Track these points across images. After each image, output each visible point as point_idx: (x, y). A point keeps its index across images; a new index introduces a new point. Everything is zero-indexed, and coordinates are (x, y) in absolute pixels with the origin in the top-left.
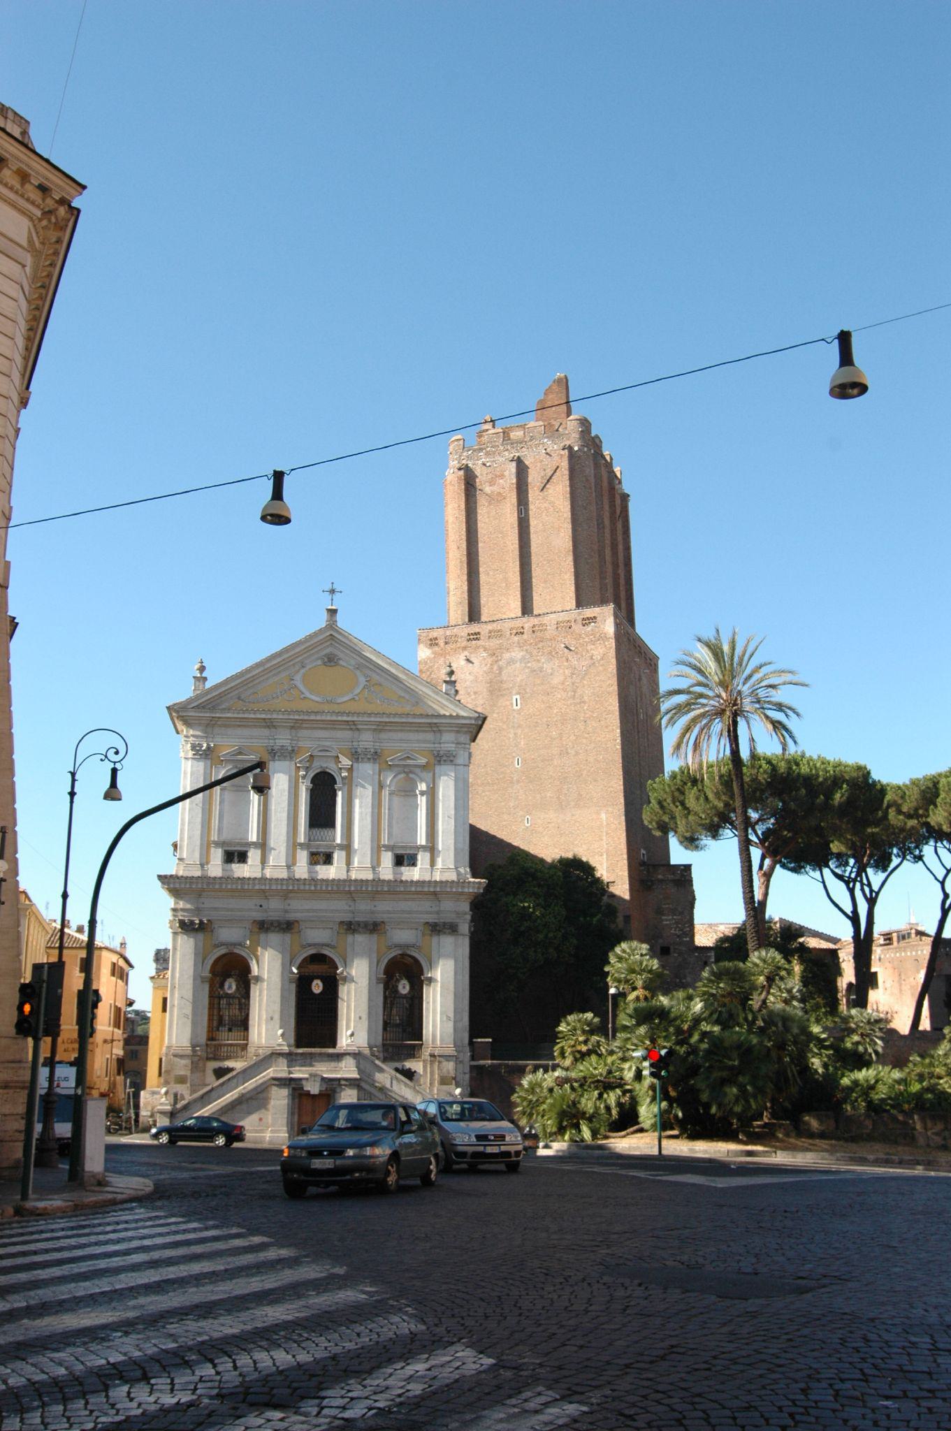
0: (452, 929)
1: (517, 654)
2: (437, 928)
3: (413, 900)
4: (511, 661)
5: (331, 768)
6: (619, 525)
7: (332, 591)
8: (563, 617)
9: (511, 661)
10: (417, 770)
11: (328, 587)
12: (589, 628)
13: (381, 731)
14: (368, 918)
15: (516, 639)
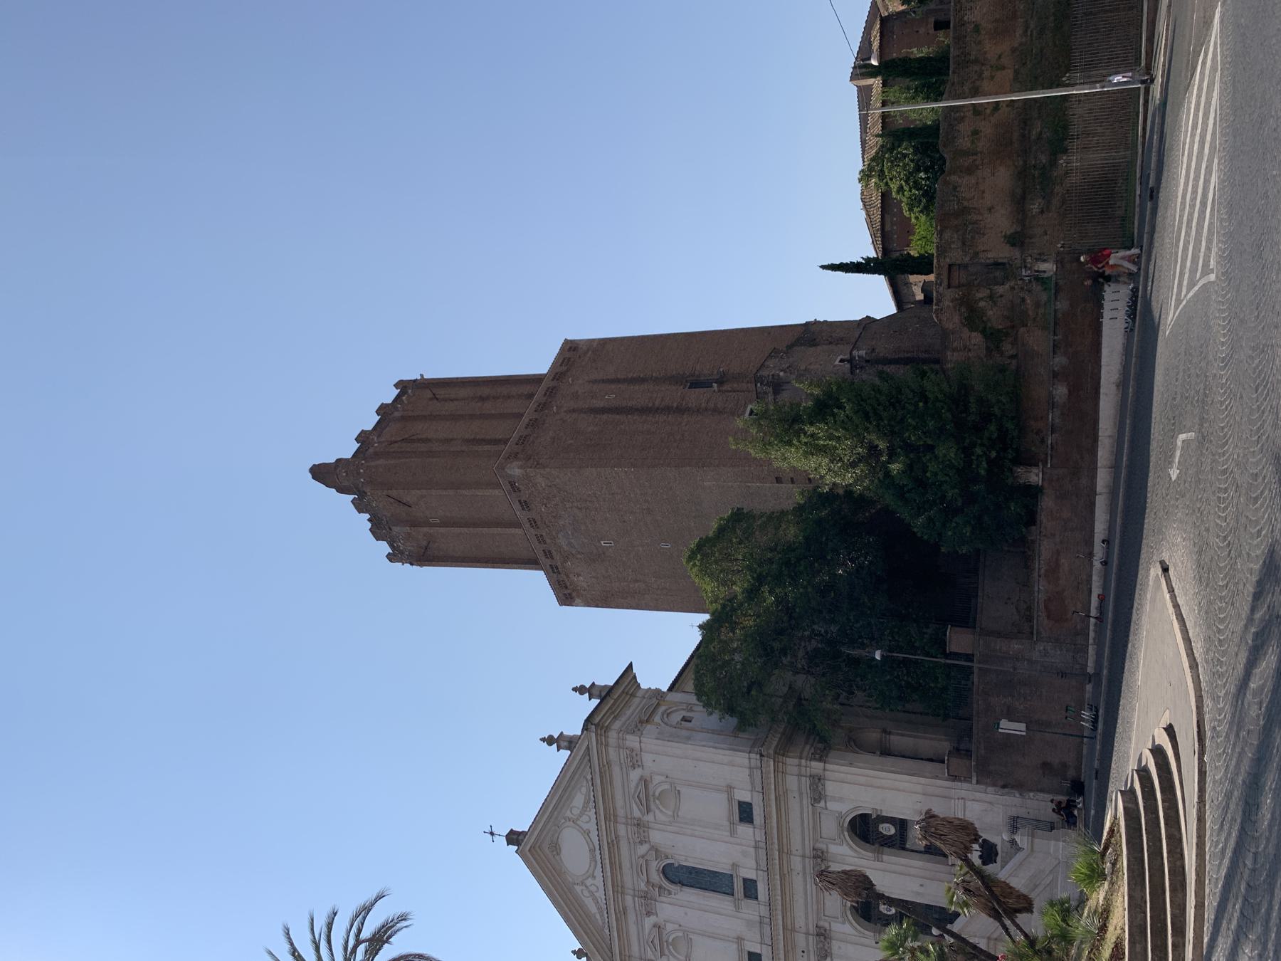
0: (817, 781)
1: (562, 542)
2: (818, 795)
3: (787, 815)
4: (570, 544)
5: (655, 866)
6: (441, 392)
7: (492, 834)
8: (516, 506)
9: (570, 544)
10: (651, 787)
11: (488, 830)
12: (522, 488)
13: (615, 816)
14: (809, 863)
15: (548, 541)
